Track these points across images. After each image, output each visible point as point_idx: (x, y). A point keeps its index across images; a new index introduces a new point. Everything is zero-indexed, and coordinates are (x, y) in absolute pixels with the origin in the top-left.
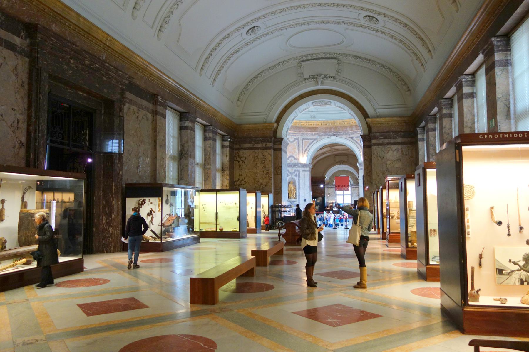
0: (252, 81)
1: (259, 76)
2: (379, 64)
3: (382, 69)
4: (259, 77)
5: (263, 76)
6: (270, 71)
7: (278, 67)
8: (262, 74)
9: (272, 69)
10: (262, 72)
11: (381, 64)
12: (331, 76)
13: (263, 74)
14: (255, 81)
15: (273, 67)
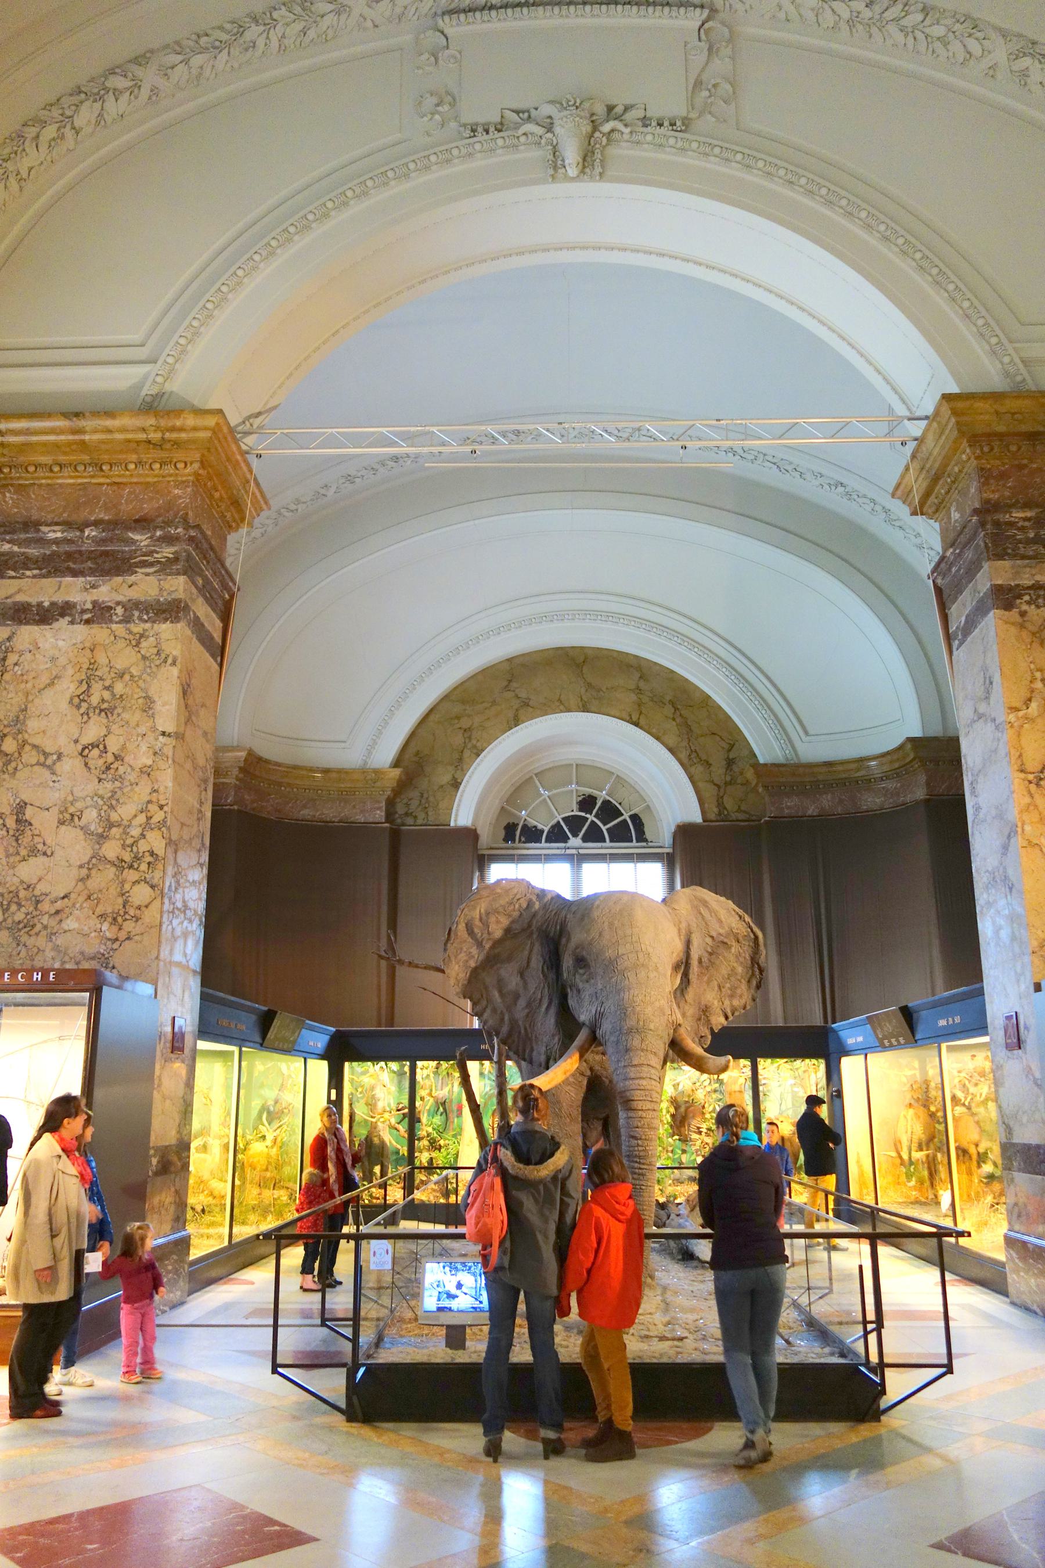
0: (56, 113)
1: (118, 82)
2: (1004, 34)
3: (1024, 74)
4: (117, 93)
5: (145, 93)
6: (197, 60)
7: (261, 42)
8: (139, 72)
9: (217, 48)
10: (140, 60)
11: (1020, 36)
12: (654, 112)
13: (149, 76)
14: (85, 116)
15: (224, 37)
